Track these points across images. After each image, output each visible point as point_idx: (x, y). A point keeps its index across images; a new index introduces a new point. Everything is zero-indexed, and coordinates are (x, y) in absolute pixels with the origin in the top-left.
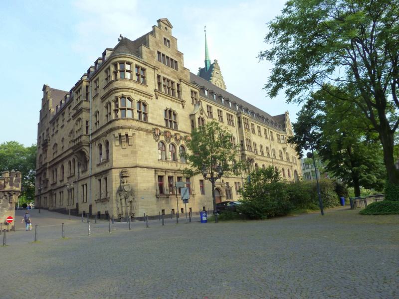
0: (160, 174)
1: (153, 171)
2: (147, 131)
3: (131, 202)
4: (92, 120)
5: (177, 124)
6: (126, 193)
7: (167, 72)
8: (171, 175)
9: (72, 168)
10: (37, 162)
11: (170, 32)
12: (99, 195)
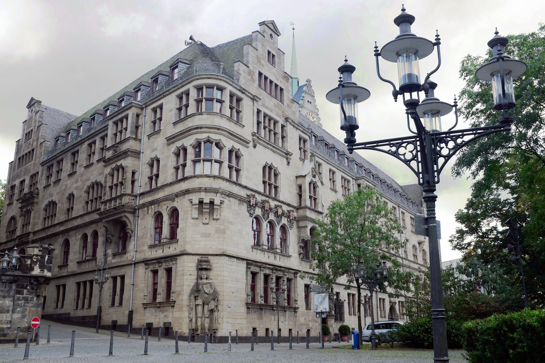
0: (254, 269)
2: (241, 200)
3: (212, 311)
4: (143, 173)
5: (279, 190)
6: (206, 296)
7: (269, 105)
11: (276, 43)
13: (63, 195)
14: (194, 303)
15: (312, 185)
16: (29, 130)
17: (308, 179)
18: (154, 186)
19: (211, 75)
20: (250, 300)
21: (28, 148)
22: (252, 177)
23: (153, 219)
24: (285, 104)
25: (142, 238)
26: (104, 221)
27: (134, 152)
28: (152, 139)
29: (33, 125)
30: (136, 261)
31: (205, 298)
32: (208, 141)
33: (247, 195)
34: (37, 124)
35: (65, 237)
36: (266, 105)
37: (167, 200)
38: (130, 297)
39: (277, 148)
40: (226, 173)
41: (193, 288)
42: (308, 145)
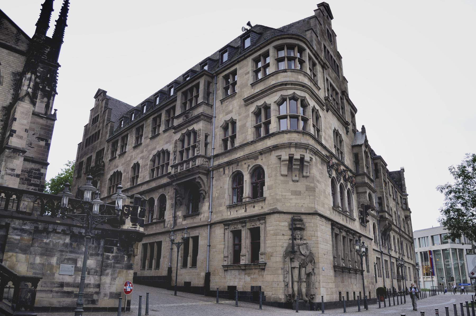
4: (218, 135)
6: (303, 257)
13: (128, 165)
16: (96, 115)
18: (229, 147)
21: (95, 130)
23: (231, 179)
25: (218, 198)
26: (174, 184)
28: (225, 103)
31: (302, 259)
37: (249, 159)
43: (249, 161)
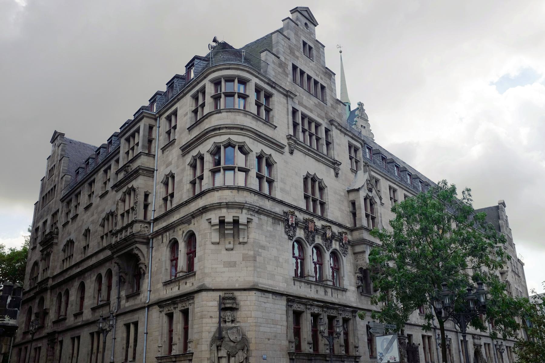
1: (282, 303)
2: (276, 218)
5: (326, 207)
6: (232, 344)
7: (307, 104)
8: (316, 312)
9: (104, 288)
10: (27, 277)
11: (312, 33)
12: (166, 347)
14: (216, 354)
15: (368, 201)
16: (53, 165)
17: (363, 194)
19: (231, 64)
20: (294, 349)
21: (51, 185)
22: (289, 188)
23: (169, 249)
24: (329, 104)
26: (115, 256)
27: (146, 170)
28: (166, 153)
29: (56, 160)
30: (150, 303)
32: (229, 144)
33: (284, 213)
34: (59, 159)
35: (81, 280)
36: (304, 103)
38: (143, 349)
39: (320, 156)
40: (254, 184)
41: (214, 335)
42: (360, 154)
43: (184, 226)
